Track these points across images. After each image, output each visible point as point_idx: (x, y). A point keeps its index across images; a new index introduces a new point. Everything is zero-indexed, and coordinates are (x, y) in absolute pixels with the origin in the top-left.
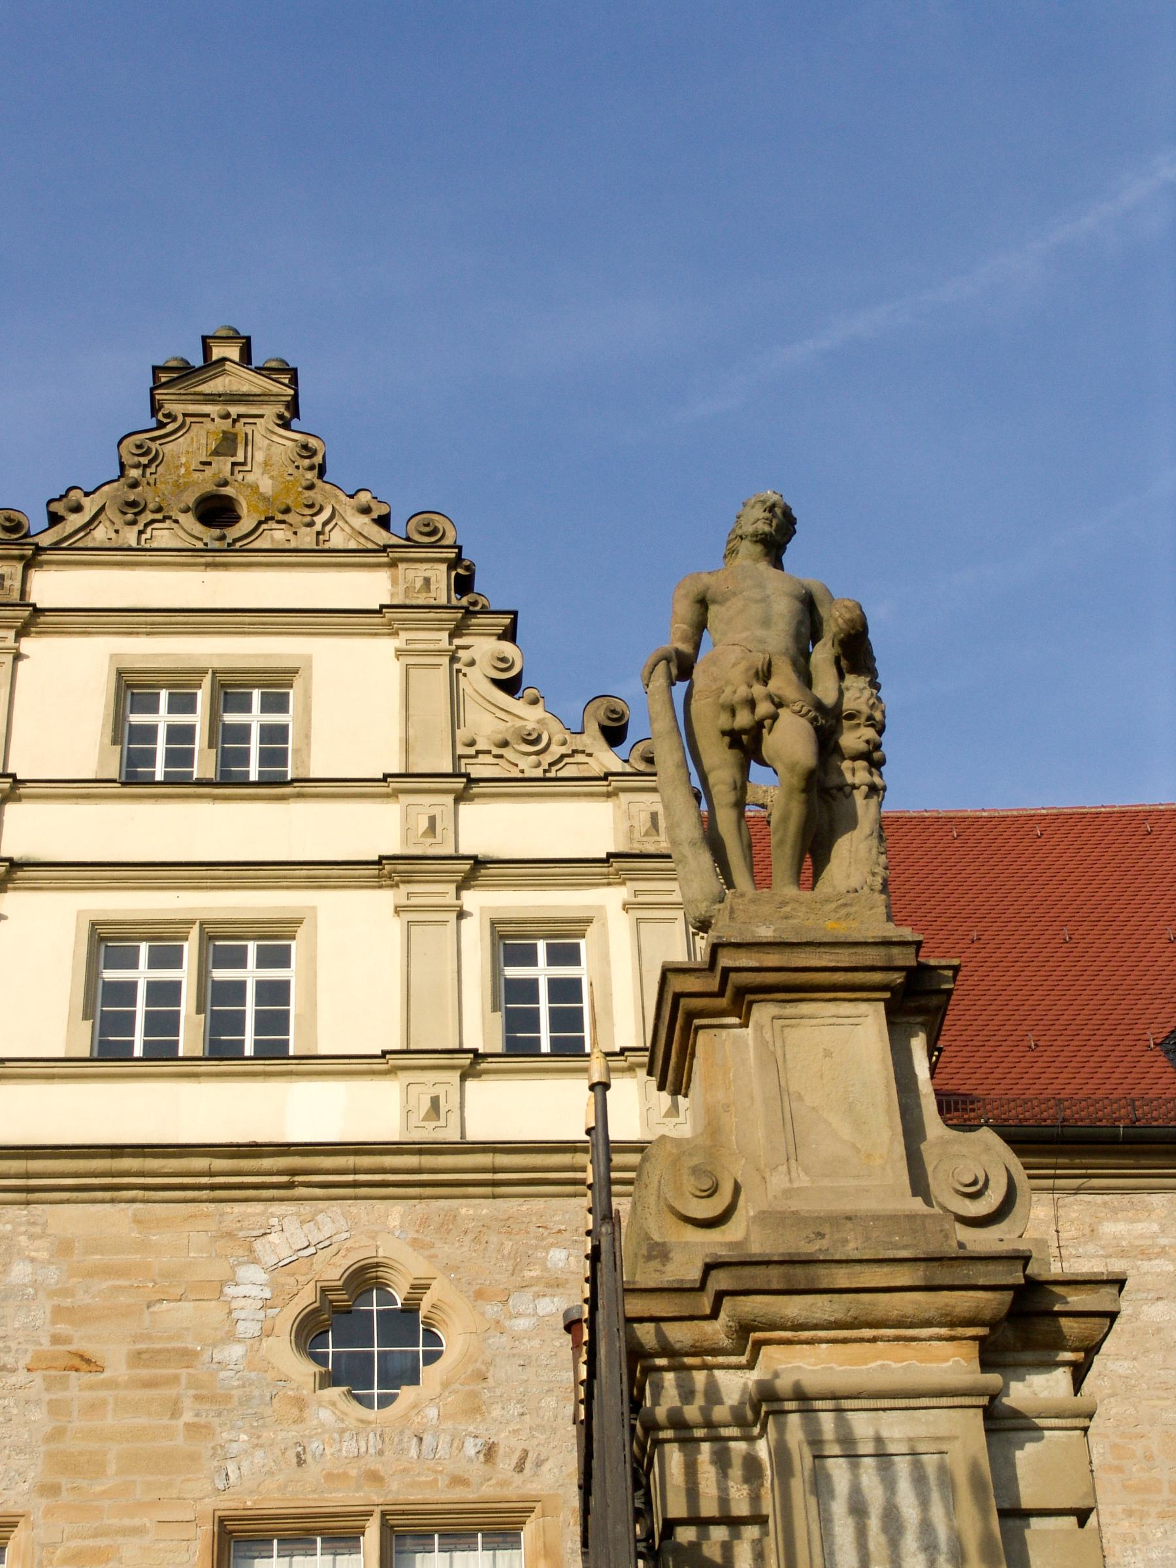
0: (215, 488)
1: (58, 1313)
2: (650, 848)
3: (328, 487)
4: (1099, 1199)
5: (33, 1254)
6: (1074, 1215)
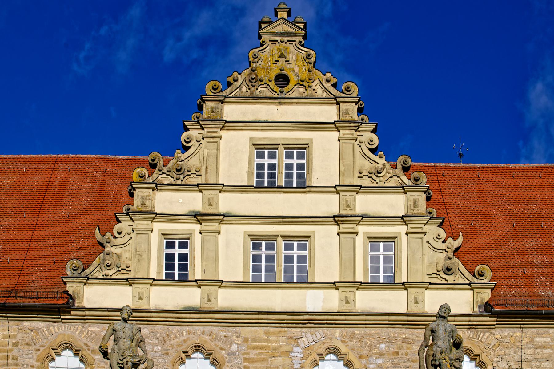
0: (280, 71)
1: (245, 359)
2: (415, 212)
3: (317, 71)
4: (535, 330)
5: (238, 342)
6: (528, 335)
